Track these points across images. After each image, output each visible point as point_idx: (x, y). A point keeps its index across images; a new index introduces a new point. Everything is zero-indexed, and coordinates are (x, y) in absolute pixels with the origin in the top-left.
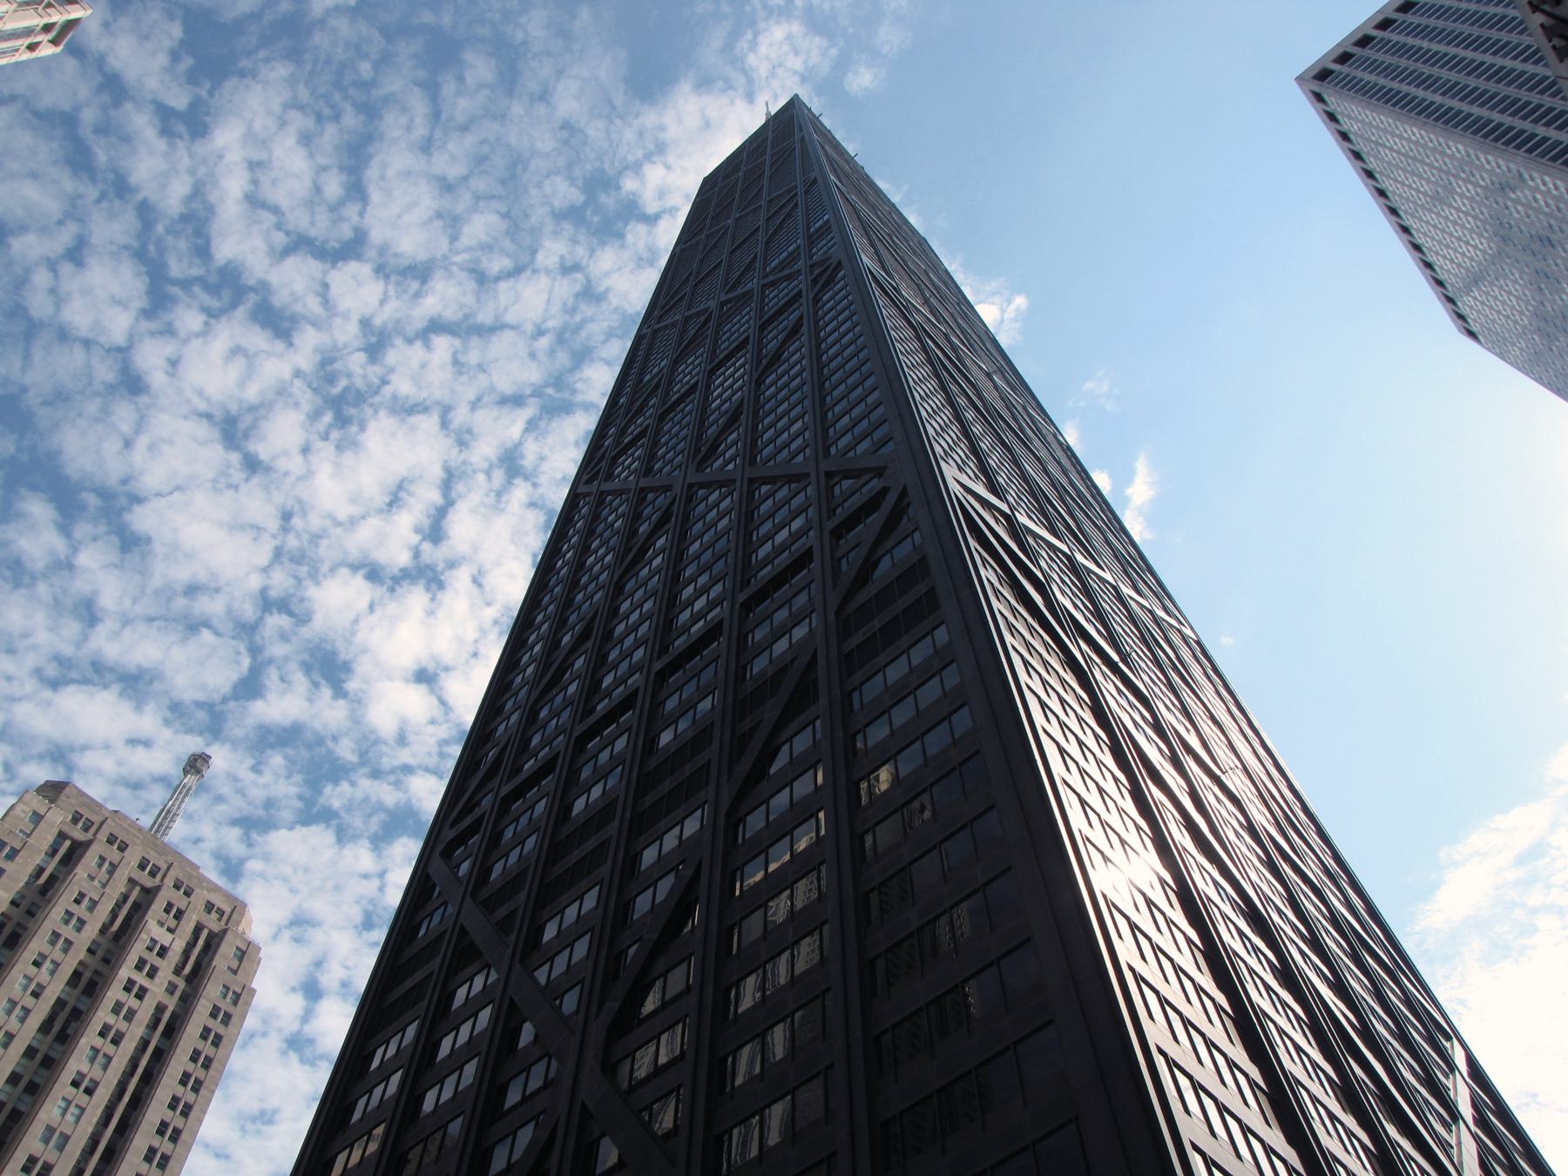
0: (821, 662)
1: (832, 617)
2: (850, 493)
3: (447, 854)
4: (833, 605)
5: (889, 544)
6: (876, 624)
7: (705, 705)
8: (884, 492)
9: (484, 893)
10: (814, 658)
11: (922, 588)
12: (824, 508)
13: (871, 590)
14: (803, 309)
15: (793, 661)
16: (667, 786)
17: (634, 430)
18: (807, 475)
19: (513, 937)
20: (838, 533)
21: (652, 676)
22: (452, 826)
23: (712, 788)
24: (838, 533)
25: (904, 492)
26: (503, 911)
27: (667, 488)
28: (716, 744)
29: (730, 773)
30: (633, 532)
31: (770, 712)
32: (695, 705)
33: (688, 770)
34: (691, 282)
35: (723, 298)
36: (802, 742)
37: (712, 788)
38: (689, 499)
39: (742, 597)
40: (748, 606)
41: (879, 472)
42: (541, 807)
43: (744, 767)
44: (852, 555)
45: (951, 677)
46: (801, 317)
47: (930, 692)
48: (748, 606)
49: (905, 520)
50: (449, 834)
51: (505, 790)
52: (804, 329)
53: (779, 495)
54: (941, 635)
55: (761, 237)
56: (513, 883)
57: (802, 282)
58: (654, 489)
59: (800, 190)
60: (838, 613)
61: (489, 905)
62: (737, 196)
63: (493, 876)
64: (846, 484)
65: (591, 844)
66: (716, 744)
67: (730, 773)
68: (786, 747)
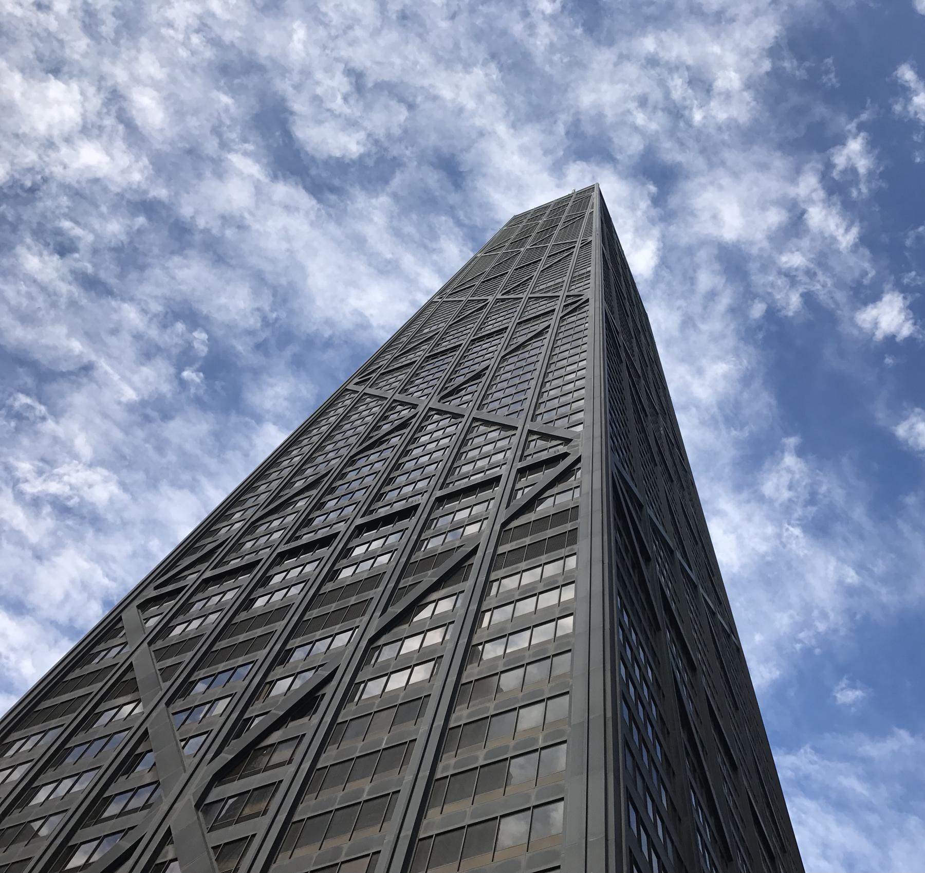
0: (480, 553)
1: (497, 527)
2: (540, 450)
3: (143, 607)
4: (502, 519)
5: (555, 490)
6: (527, 541)
7: (384, 559)
8: (565, 455)
9: (159, 644)
10: (474, 551)
11: (569, 526)
12: (519, 453)
13: (531, 517)
14: (552, 322)
15: (459, 547)
16: (333, 607)
17: (404, 361)
18: (516, 428)
19: (169, 683)
20: (522, 472)
21: (353, 527)
22: (156, 588)
23: (366, 618)
24: (522, 472)
25: (579, 460)
26: (169, 662)
27: (415, 406)
28: (381, 588)
29: (384, 610)
30: (377, 428)
31: (430, 577)
32: (376, 554)
33: (353, 600)
34: (482, 279)
35: (499, 296)
36: (445, 606)
37: (366, 618)
38: (427, 417)
39: (438, 494)
40: (440, 501)
41: (567, 441)
42: (229, 596)
43: (396, 609)
44: (526, 490)
45: (568, 594)
46: (548, 327)
47: (549, 599)
48: (440, 501)
49: (573, 478)
50: (151, 593)
51: (208, 574)
52: (548, 336)
53: (491, 435)
54: (572, 562)
55: (540, 267)
56: (184, 644)
57: (558, 305)
58: (402, 403)
59: (578, 245)
60: (504, 525)
61: (161, 654)
62: (533, 235)
63: (173, 634)
64: (541, 443)
65: (259, 632)
66: (381, 588)
67: (384, 610)
68: (432, 606)
